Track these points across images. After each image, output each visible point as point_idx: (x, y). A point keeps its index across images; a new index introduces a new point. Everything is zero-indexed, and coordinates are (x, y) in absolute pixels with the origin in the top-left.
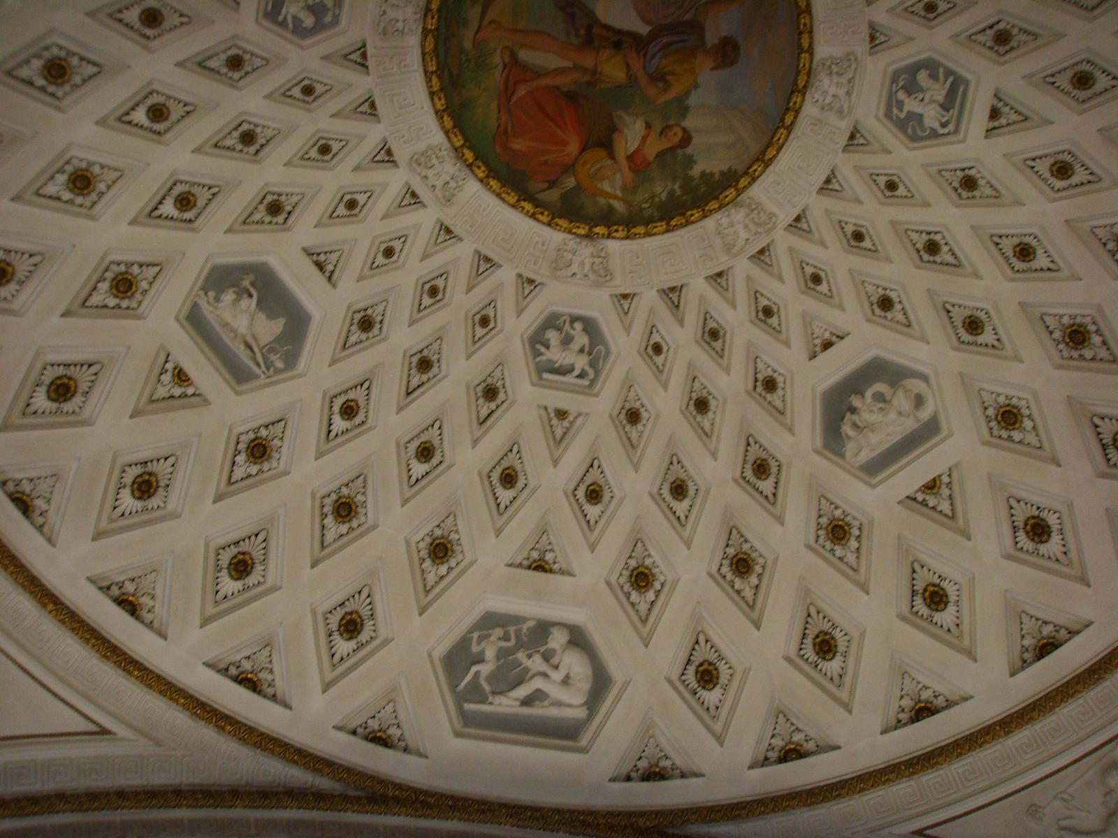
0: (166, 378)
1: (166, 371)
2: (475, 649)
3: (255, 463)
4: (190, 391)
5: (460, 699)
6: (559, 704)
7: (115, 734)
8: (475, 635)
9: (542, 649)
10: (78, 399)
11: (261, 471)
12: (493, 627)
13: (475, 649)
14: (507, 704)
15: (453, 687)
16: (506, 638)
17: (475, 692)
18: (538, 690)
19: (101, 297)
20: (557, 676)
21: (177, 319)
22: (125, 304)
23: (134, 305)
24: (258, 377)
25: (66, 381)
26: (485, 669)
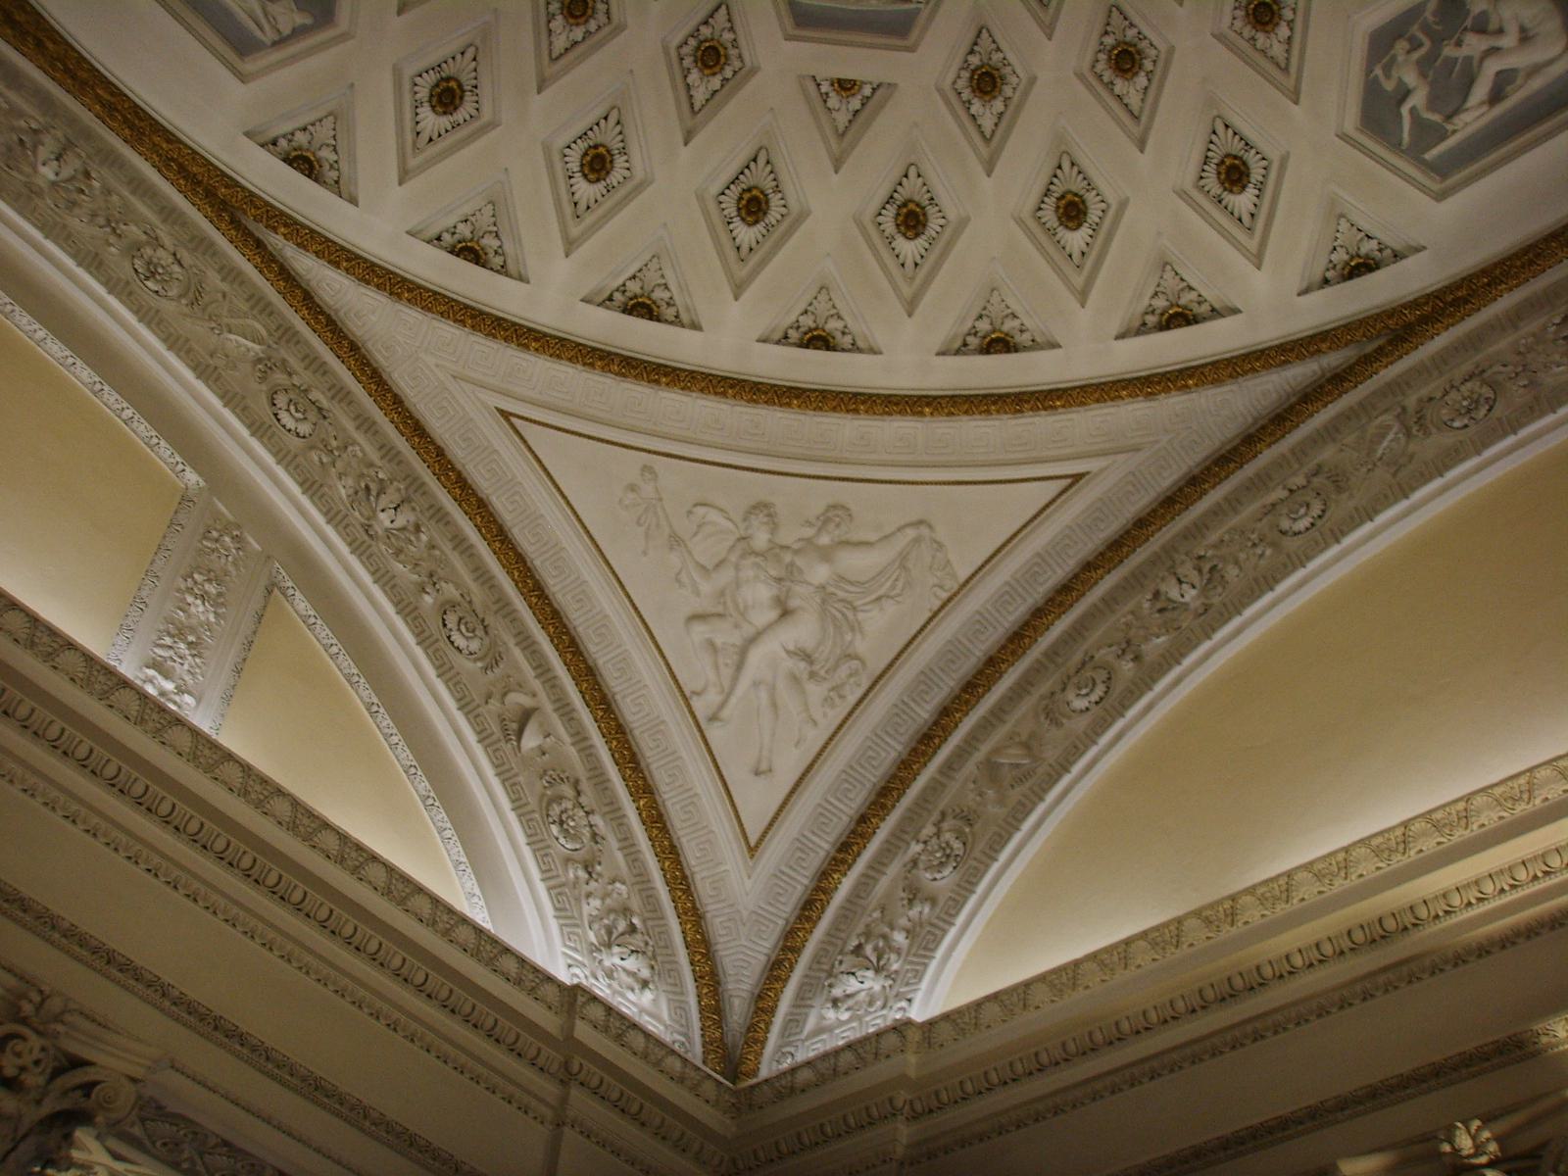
0: (834, 101)
1: (827, 94)
2: (1389, 86)
4: (867, 91)
5: (1415, 153)
6: (1534, 70)
7: (1088, 473)
8: (1378, 71)
9: (1468, 23)
10: (775, 200)
11: (1007, 100)
12: (1391, 46)
13: (1389, 86)
14: (1473, 118)
15: (1396, 146)
16: (1415, 45)
17: (1427, 133)
18: (1499, 73)
19: (702, 89)
20: (1508, 41)
21: (788, 38)
22: (728, 72)
23: (737, 64)
24: (918, 11)
25: (747, 196)
26: (1418, 99)
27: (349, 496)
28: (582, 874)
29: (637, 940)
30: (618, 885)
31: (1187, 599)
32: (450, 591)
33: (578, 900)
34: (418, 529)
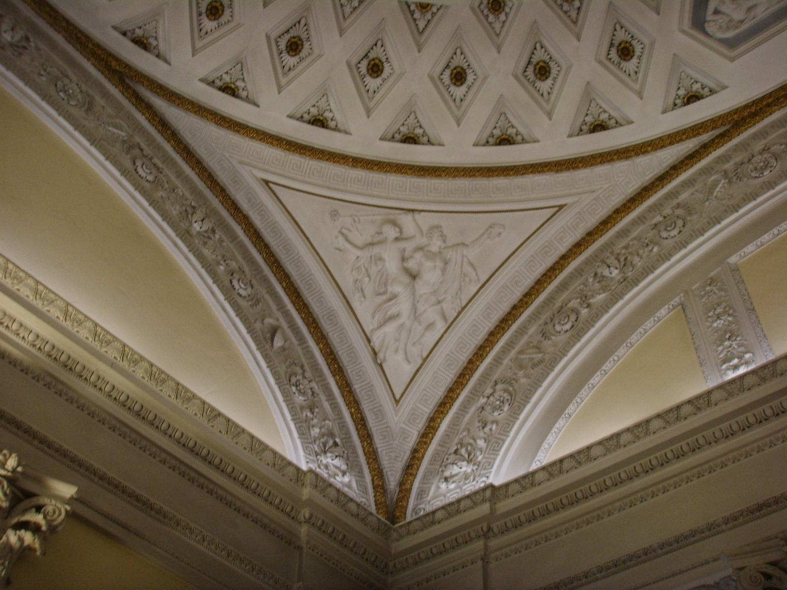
3: (501, 13)
28: (309, 414)
29: (338, 451)
30: (327, 422)
34: (213, 231)
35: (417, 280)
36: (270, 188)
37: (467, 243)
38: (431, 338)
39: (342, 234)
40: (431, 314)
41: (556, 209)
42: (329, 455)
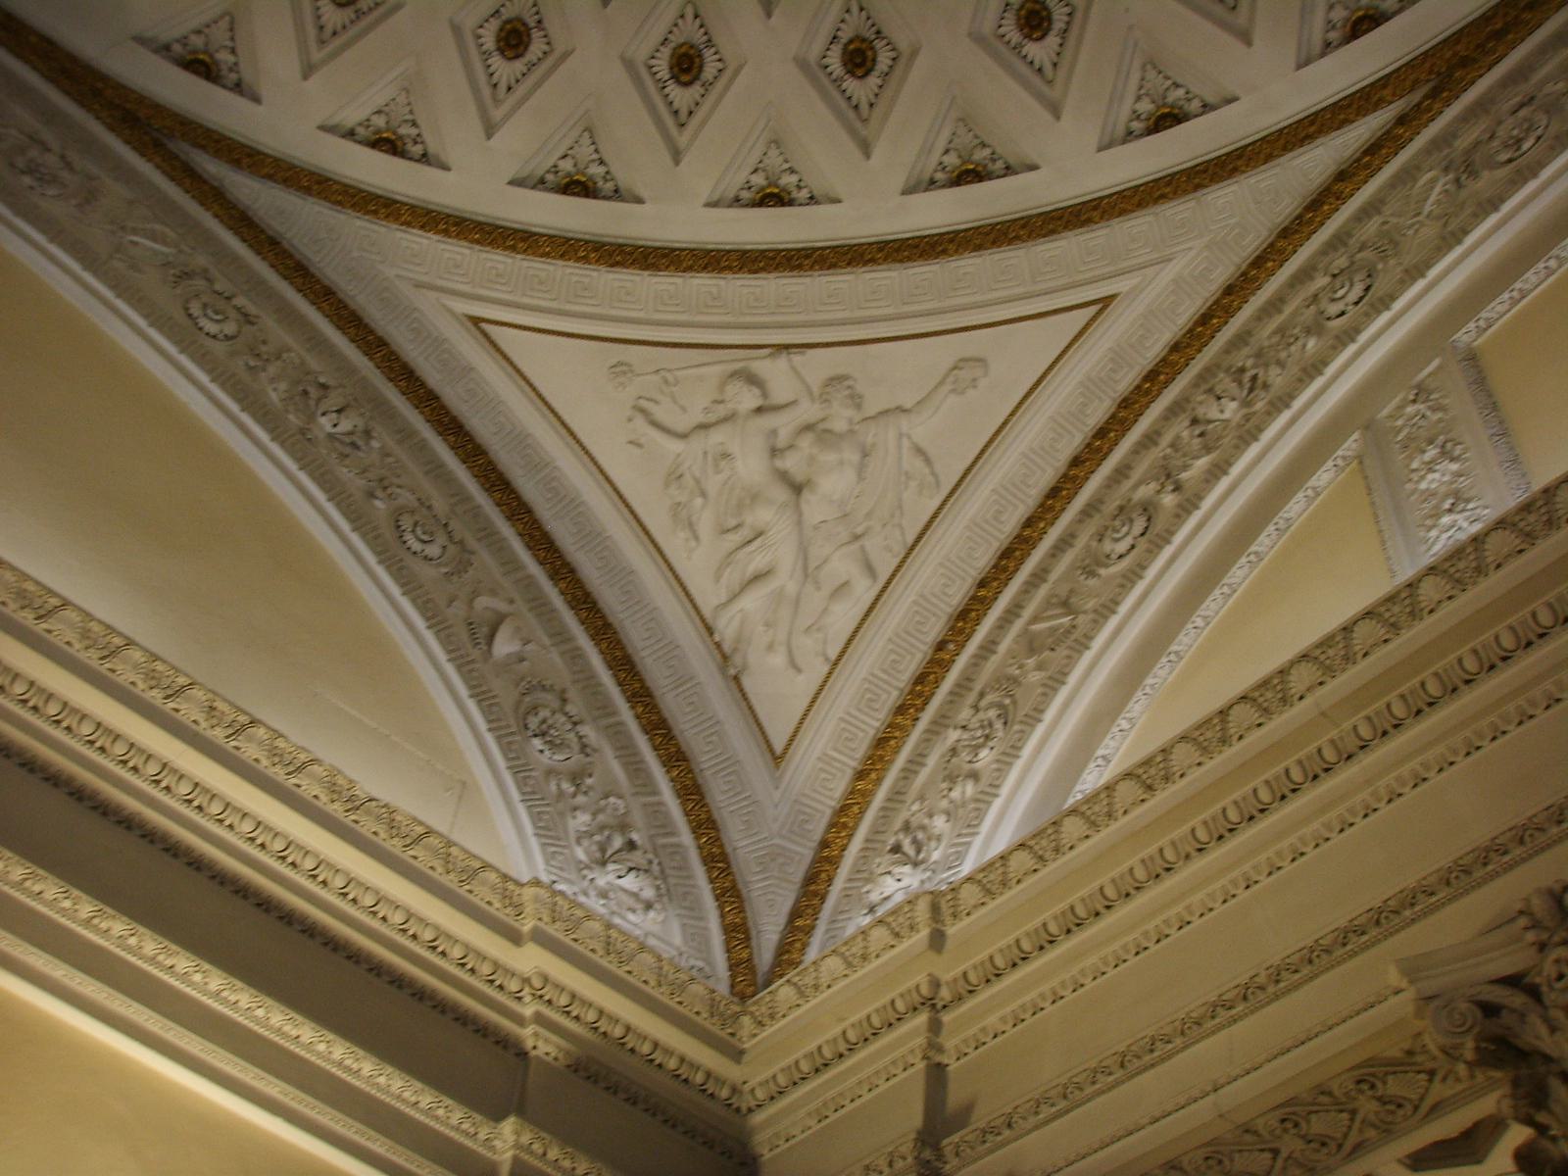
27: (282, 400)
29: (637, 858)
30: (612, 800)
31: (1227, 415)
32: (406, 498)
33: (562, 814)
34: (368, 434)
35: (806, 495)
36: (486, 335)
37: (908, 405)
38: (843, 616)
39: (643, 411)
40: (842, 565)
41: (1093, 309)
42: (611, 867)
